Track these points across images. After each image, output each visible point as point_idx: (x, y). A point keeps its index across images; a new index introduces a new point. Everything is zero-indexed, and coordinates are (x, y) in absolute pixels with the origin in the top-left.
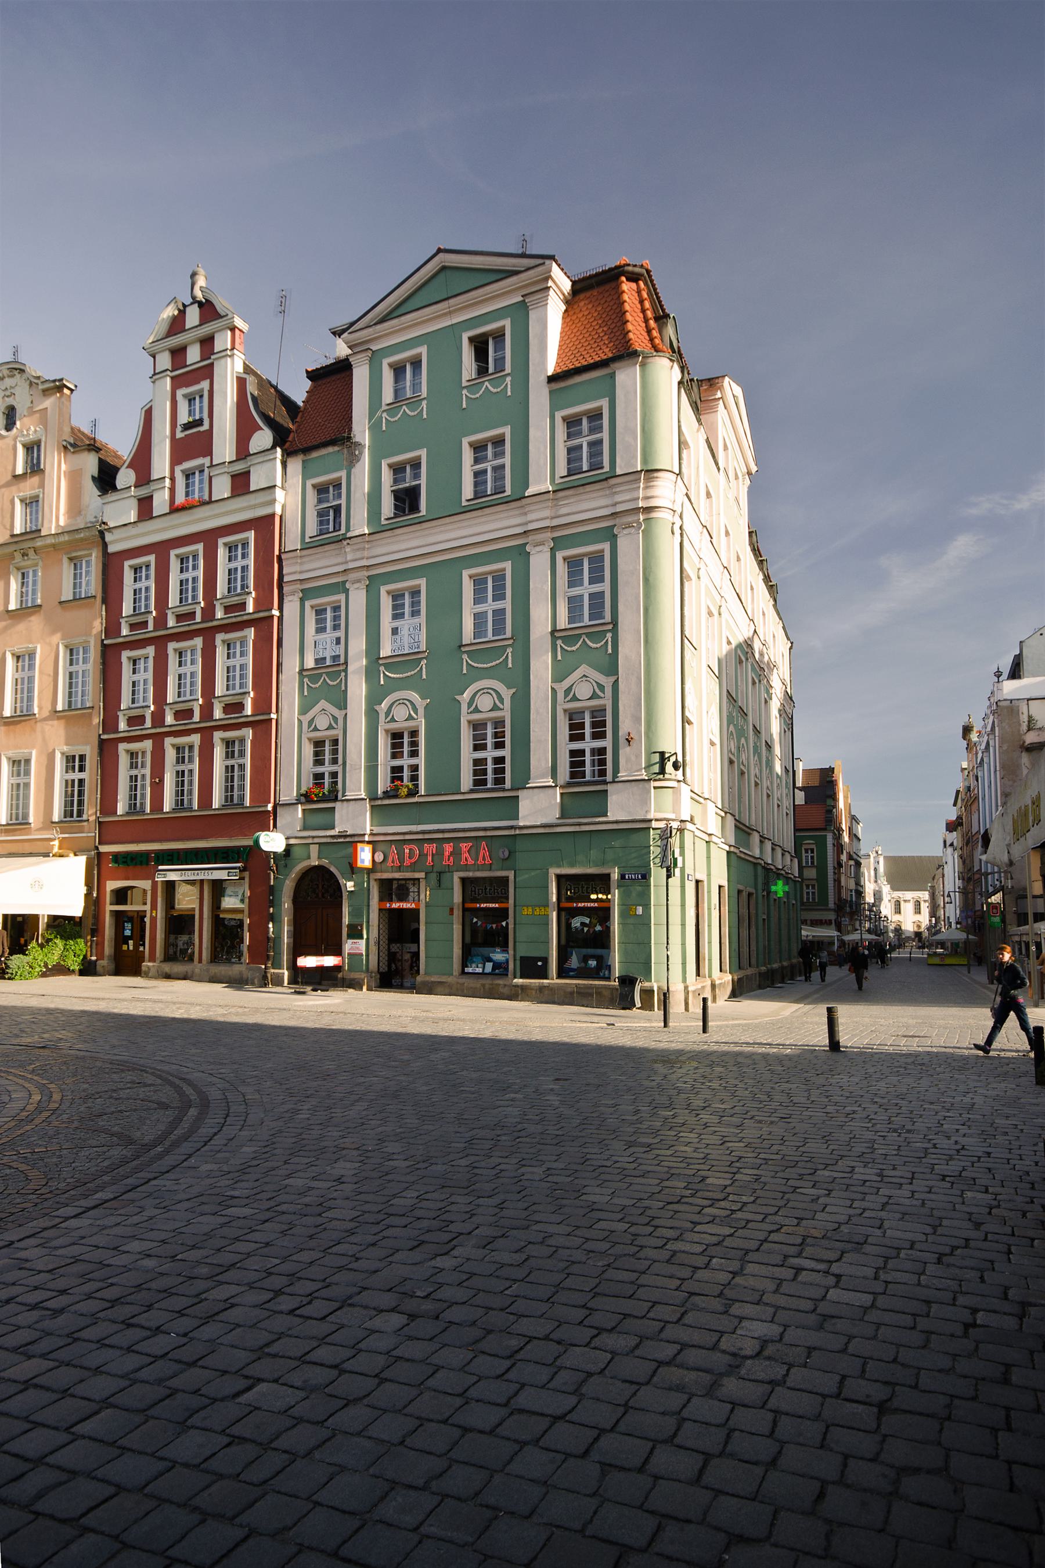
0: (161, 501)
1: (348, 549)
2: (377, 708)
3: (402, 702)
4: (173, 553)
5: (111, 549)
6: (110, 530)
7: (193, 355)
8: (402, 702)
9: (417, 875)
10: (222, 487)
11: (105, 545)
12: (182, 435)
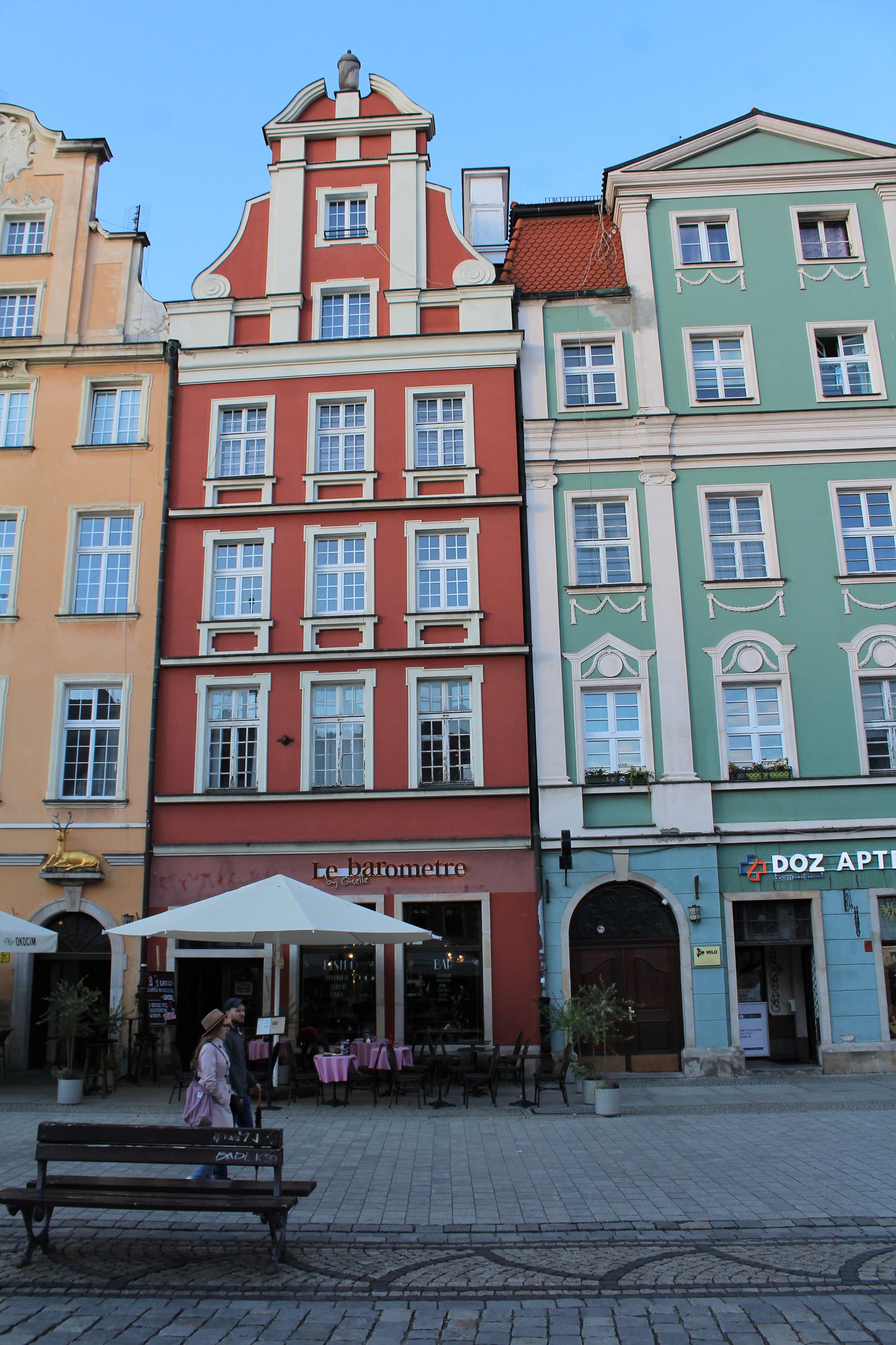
0: (283, 324)
1: (643, 430)
2: (709, 651)
3: (747, 645)
4: (410, 392)
5: (183, 378)
6: (189, 351)
7: (347, 150)
8: (747, 645)
9: (805, 895)
10: (404, 319)
11: (175, 370)
12: (328, 244)
